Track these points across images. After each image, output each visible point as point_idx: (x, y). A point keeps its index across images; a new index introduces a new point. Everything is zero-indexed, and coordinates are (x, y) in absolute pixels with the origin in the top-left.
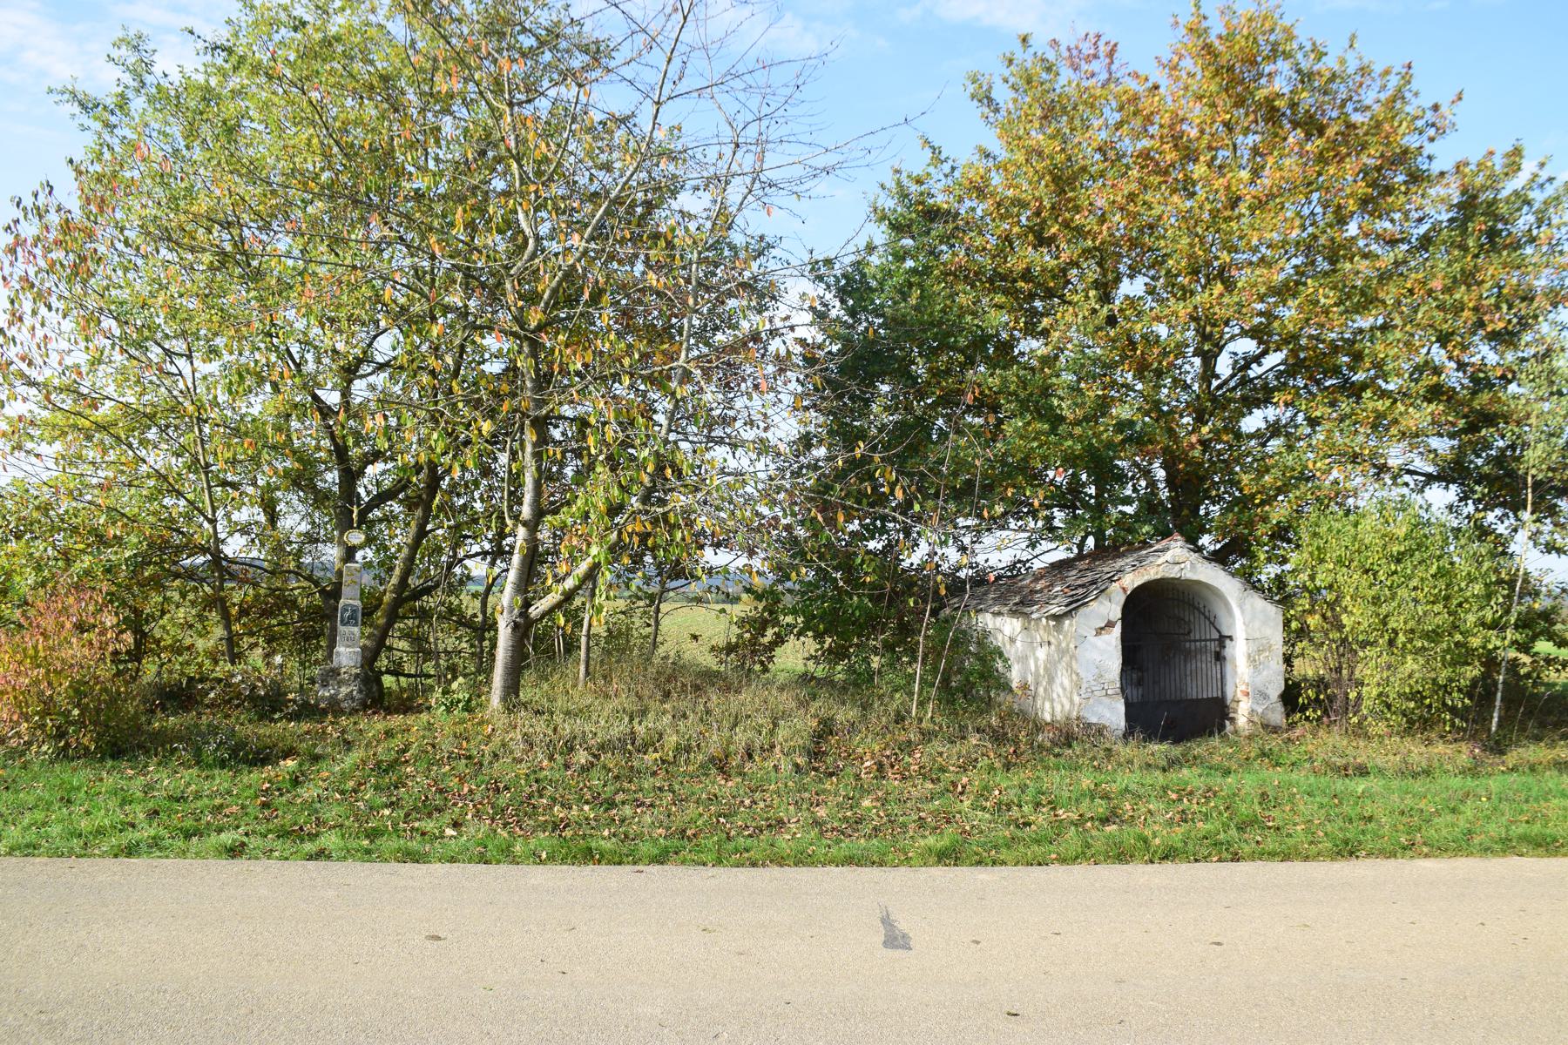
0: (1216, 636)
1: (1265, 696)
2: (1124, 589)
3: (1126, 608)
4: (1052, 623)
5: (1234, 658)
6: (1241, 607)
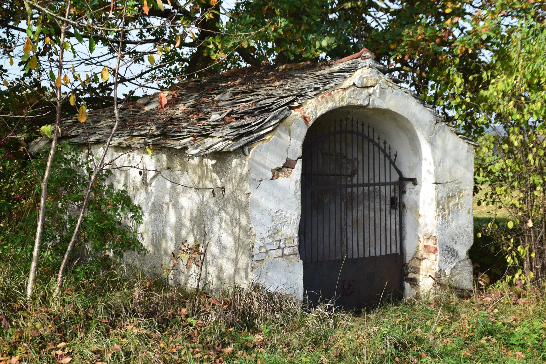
0: (395, 178)
1: (451, 252)
2: (305, 118)
3: (306, 145)
4: (210, 162)
5: (416, 206)
6: (431, 142)
